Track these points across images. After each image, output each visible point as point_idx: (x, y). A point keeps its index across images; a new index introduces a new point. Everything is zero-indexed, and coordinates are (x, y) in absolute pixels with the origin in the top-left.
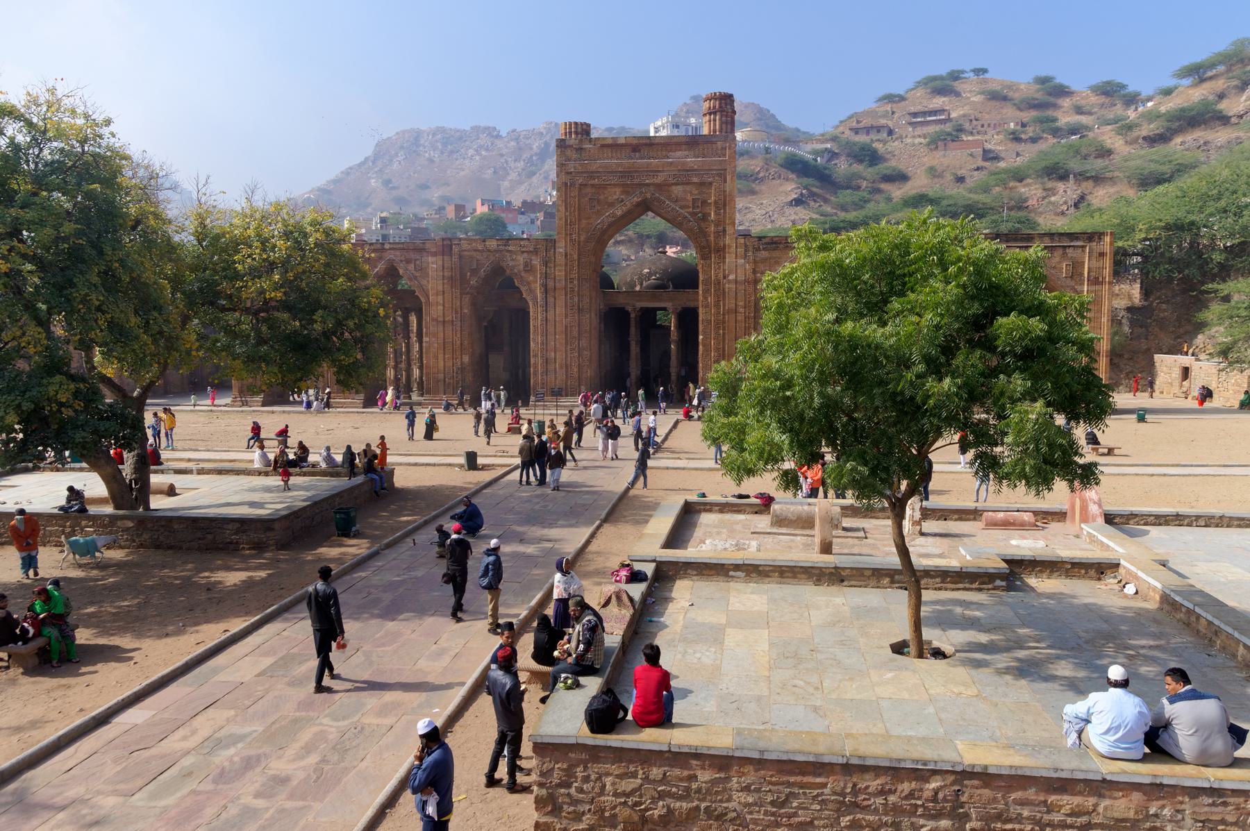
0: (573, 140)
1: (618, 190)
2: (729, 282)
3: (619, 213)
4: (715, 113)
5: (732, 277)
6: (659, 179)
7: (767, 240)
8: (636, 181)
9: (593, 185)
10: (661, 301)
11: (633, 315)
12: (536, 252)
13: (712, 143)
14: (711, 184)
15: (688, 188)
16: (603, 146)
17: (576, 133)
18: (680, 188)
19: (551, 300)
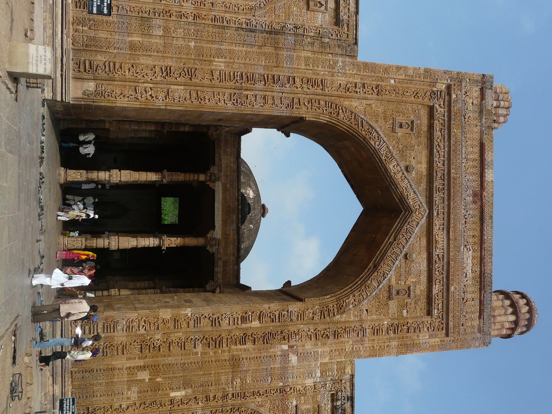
0: (490, 102)
1: (423, 167)
2: (285, 355)
3: (391, 167)
4: (515, 312)
5: (294, 359)
6: (440, 236)
7: (349, 410)
8: (437, 198)
9: (431, 127)
10: (225, 223)
11: (202, 177)
12: (337, 22)
13: (481, 312)
14: (429, 313)
15: (424, 278)
16: (482, 146)
17: (498, 107)
18: (424, 266)
19: (260, 38)
